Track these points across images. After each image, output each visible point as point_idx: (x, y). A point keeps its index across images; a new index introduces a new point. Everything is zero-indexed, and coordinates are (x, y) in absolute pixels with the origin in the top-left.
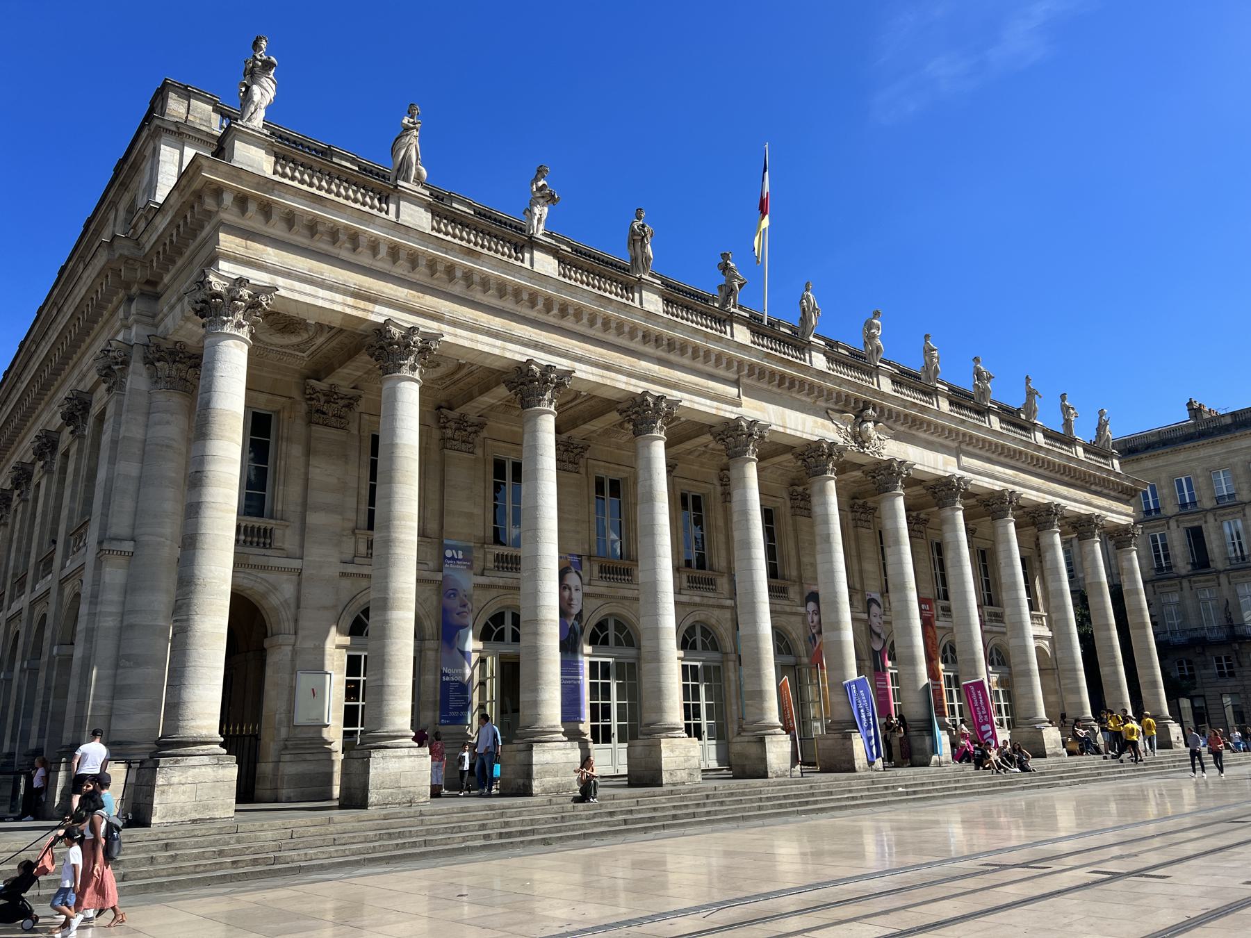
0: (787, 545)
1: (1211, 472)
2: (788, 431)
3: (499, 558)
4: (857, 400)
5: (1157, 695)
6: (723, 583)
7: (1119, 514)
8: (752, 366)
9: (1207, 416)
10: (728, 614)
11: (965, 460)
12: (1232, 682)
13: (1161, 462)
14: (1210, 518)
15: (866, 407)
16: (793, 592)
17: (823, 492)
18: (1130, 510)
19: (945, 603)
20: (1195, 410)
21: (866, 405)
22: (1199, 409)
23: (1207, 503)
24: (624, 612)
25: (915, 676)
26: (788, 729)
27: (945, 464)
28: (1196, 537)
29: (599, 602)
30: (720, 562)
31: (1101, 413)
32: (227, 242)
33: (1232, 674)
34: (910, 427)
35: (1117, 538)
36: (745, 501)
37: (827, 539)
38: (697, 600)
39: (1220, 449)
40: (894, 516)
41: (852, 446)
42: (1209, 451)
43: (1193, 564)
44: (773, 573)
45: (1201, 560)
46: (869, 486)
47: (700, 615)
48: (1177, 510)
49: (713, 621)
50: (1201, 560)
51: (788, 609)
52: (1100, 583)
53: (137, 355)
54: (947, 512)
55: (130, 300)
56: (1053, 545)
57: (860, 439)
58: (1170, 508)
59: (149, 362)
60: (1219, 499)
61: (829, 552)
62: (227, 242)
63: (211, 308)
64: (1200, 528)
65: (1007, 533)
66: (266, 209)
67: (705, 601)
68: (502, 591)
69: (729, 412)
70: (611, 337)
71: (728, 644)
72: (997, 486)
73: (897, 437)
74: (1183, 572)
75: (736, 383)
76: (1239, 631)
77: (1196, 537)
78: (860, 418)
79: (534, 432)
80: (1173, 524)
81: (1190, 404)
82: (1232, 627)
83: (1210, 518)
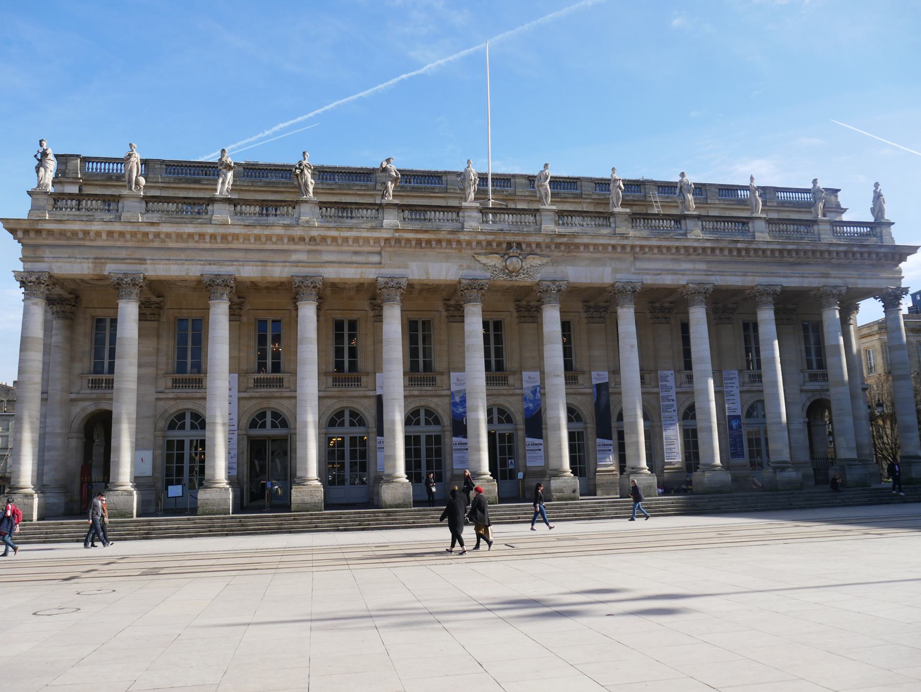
2: (431, 278)
4: (499, 244)
8: (387, 240)
19: (688, 372)
24: (354, 406)
27: (615, 271)
29: (333, 401)
31: (877, 185)
38: (416, 393)
49: (432, 405)
51: (505, 392)
52: (838, 346)
66: (39, 232)
67: (423, 393)
68: (260, 400)
72: (682, 280)
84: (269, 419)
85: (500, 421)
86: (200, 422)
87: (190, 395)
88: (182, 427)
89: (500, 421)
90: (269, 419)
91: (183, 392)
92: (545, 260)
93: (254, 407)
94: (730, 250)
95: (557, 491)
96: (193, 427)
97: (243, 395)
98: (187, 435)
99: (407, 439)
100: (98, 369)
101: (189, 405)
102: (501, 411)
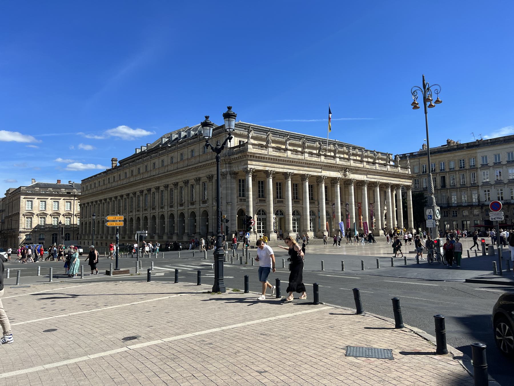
0: (330, 194)
1: (449, 161)
3: (278, 201)
5: (411, 223)
6: (316, 203)
7: (408, 183)
9: (452, 145)
10: (317, 209)
11: (368, 176)
12: (447, 218)
13: (437, 157)
14: (447, 174)
15: (347, 168)
16: (330, 204)
17: (337, 187)
18: (411, 181)
20: (449, 142)
21: (347, 168)
22: (450, 143)
23: (447, 170)
25: (353, 221)
26: (328, 231)
28: (443, 178)
30: (316, 198)
32: (249, 162)
33: (447, 216)
34: (356, 171)
35: (408, 187)
36: (322, 191)
37: (337, 196)
39: (452, 155)
40: (351, 190)
41: (343, 177)
42: (450, 155)
43: (442, 187)
44: (326, 200)
45: (444, 186)
46: (346, 183)
47: (312, 209)
48: (439, 171)
50: (444, 186)
53: (228, 173)
54: (363, 187)
55: (226, 164)
56: (388, 192)
57: (345, 175)
58: (438, 171)
59: (230, 174)
60: (450, 169)
61: (337, 199)
62: (249, 162)
63: (247, 172)
64: (444, 177)
65: (377, 190)
66: (254, 156)
69: (319, 174)
70: (300, 165)
71: (317, 214)
72: (375, 180)
73: (353, 174)
74: (439, 188)
75: (321, 168)
76: (450, 205)
77: (443, 178)
78: (345, 171)
79: (288, 184)
80: (438, 175)
81: (448, 140)
82: (449, 204)
83: (447, 174)
91: (262, 204)
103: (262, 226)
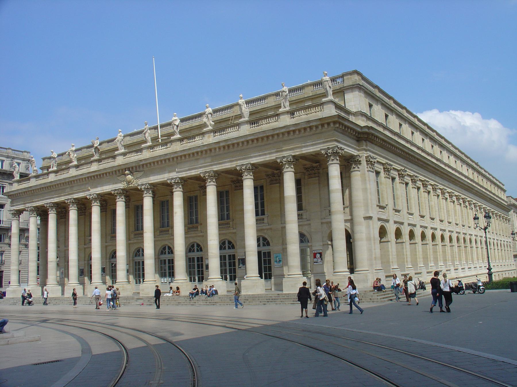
2: (104, 191)
38: (135, 241)
84: (196, 248)
85: (264, 245)
86: (171, 251)
87: (163, 238)
88: (193, 251)
89: (264, 245)
90: (196, 248)
92: (142, 173)
93: (161, 244)
94: (219, 148)
95: (143, 290)
96: (169, 253)
97: (187, 236)
98: (167, 257)
99: (222, 258)
100: (137, 229)
101: (166, 243)
102: (265, 239)
103: (228, 268)
